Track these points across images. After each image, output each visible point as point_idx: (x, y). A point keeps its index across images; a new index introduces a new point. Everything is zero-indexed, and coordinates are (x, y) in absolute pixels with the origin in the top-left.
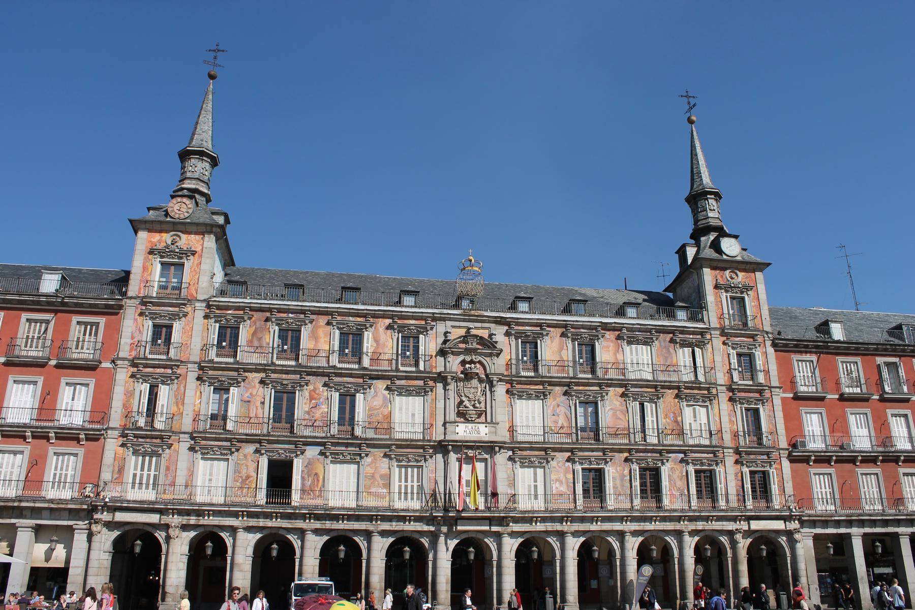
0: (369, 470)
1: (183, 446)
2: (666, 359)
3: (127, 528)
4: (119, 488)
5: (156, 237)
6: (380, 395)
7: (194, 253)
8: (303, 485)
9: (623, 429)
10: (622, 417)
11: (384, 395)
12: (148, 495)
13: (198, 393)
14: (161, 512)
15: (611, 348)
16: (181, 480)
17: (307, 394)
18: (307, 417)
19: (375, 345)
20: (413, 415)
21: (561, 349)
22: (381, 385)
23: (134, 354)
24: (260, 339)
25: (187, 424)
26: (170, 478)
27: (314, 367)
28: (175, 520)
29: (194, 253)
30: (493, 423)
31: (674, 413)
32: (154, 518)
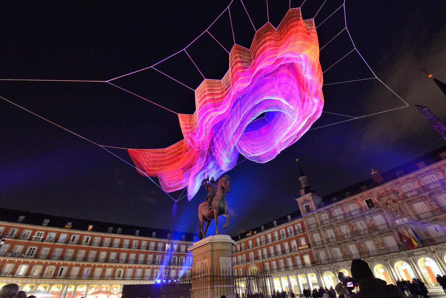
1: (327, 248)
11: (370, 219)
16: (331, 257)
18: (352, 232)
19: (359, 206)
21: (419, 182)
24: (332, 215)
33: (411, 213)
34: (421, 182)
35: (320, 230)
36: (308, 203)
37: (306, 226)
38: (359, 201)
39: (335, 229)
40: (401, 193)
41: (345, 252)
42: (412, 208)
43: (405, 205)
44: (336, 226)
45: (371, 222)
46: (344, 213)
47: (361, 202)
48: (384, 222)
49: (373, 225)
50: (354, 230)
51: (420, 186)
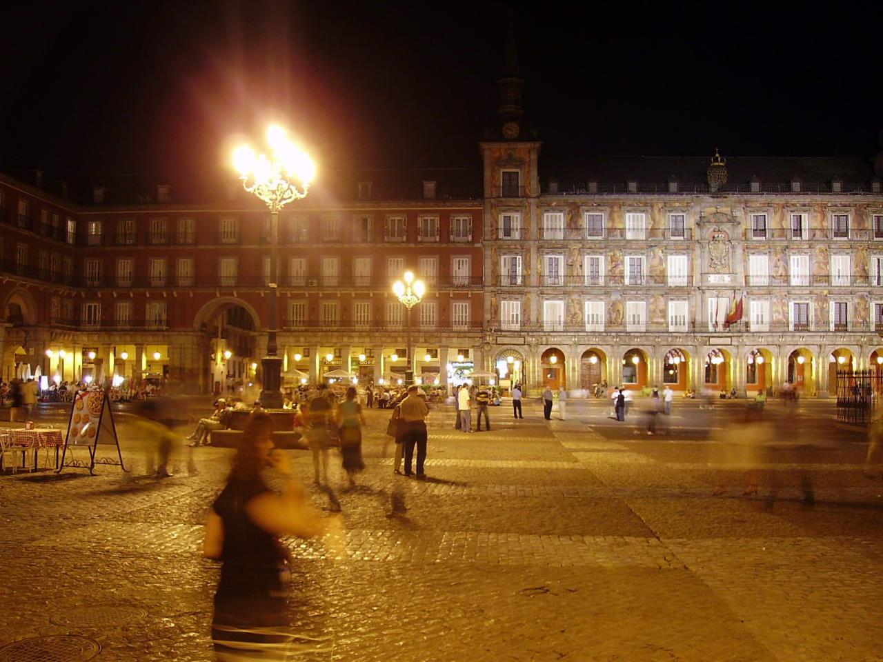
0: (652, 307)
2: (859, 225)
8: (610, 317)
9: (825, 276)
10: (824, 267)
11: (660, 258)
13: (539, 261)
15: (819, 218)
16: (533, 318)
17: (610, 258)
18: (610, 274)
19: (652, 222)
20: (680, 270)
26: (526, 316)
30: (733, 273)
31: (863, 264)
33: (739, 269)
34: (785, 218)
35: (528, 251)
36: (517, 167)
37: (487, 228)
38: (656, 211)
39: (572, 258)
40: (745, 227)
42: (745, 261)
43: (739, 251)
44: (576, 252)
45: (662, 265)
47: (659, 214)
50: (617, 272)
51: (779, 227)
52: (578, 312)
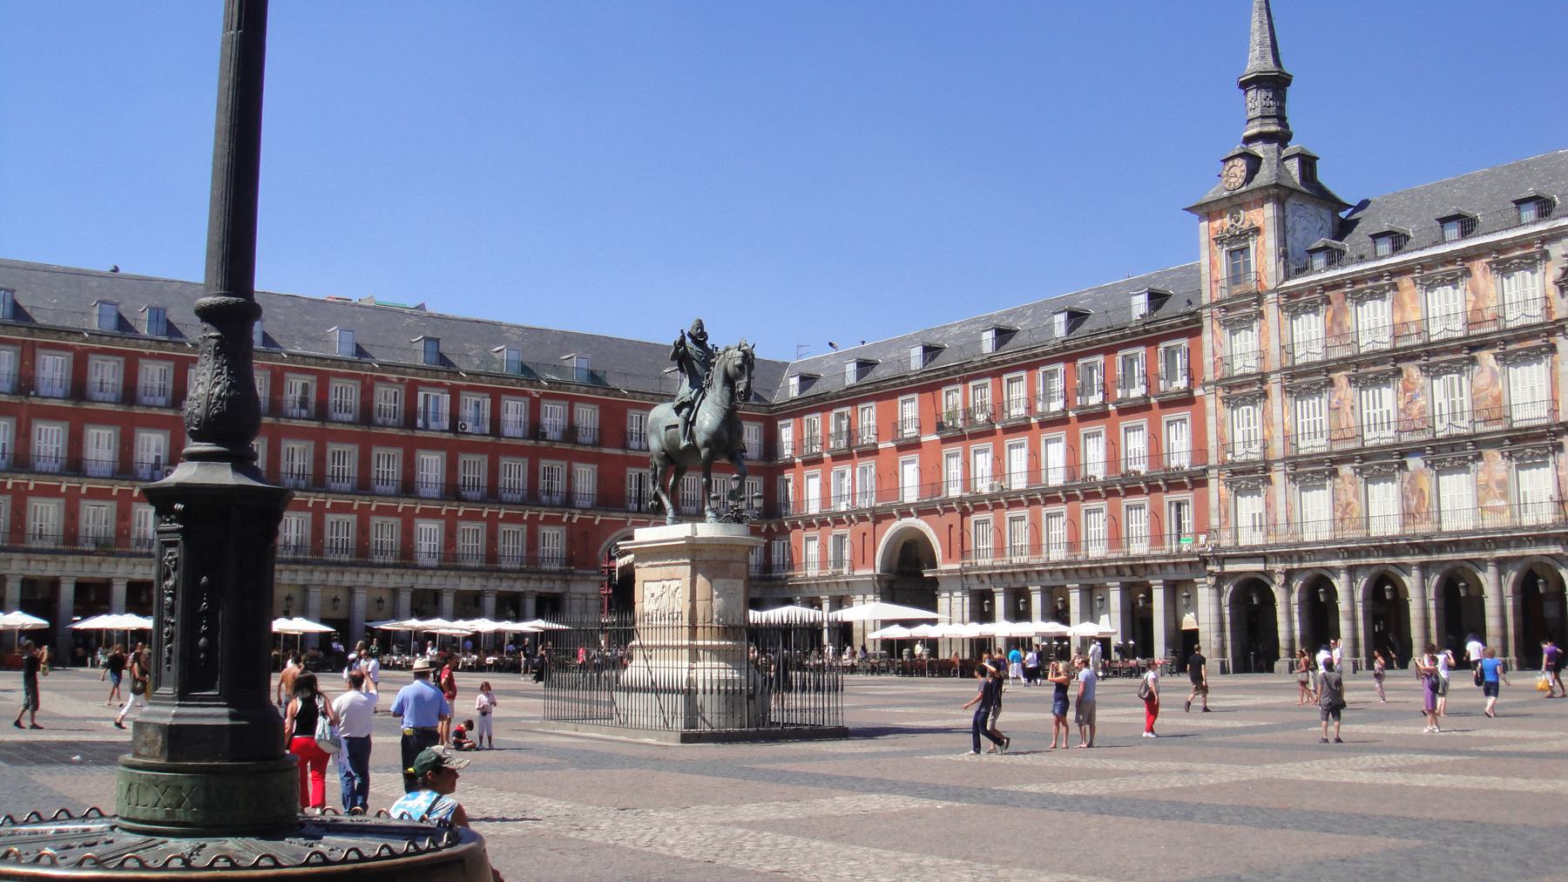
3: (1241, 578)
4: (1227, 534)
5: (1217, 224)
6: (1487, 369)
7: (1257, 231)
11: (1493, 371)
12: (1258, 539)
14: (1265, 558)
16: (1281, 518)
18: (1402, 416)
19: (1471, 297)
20: (1533, 389)
22: (1487, 357)
23: (1219, 374)
24: (1340, 324)
25: (1277, 450)
27: (1406, 348)
28: (1279, 567)
29: (1257, 231)
32: (1259, 567)
37: (1208, 360)
41: (1348, 504)
44: (1344, 381)
46: (1397, 319)
48: (1543, 393)
49: (1497, 399)
52: (1353, 500)
